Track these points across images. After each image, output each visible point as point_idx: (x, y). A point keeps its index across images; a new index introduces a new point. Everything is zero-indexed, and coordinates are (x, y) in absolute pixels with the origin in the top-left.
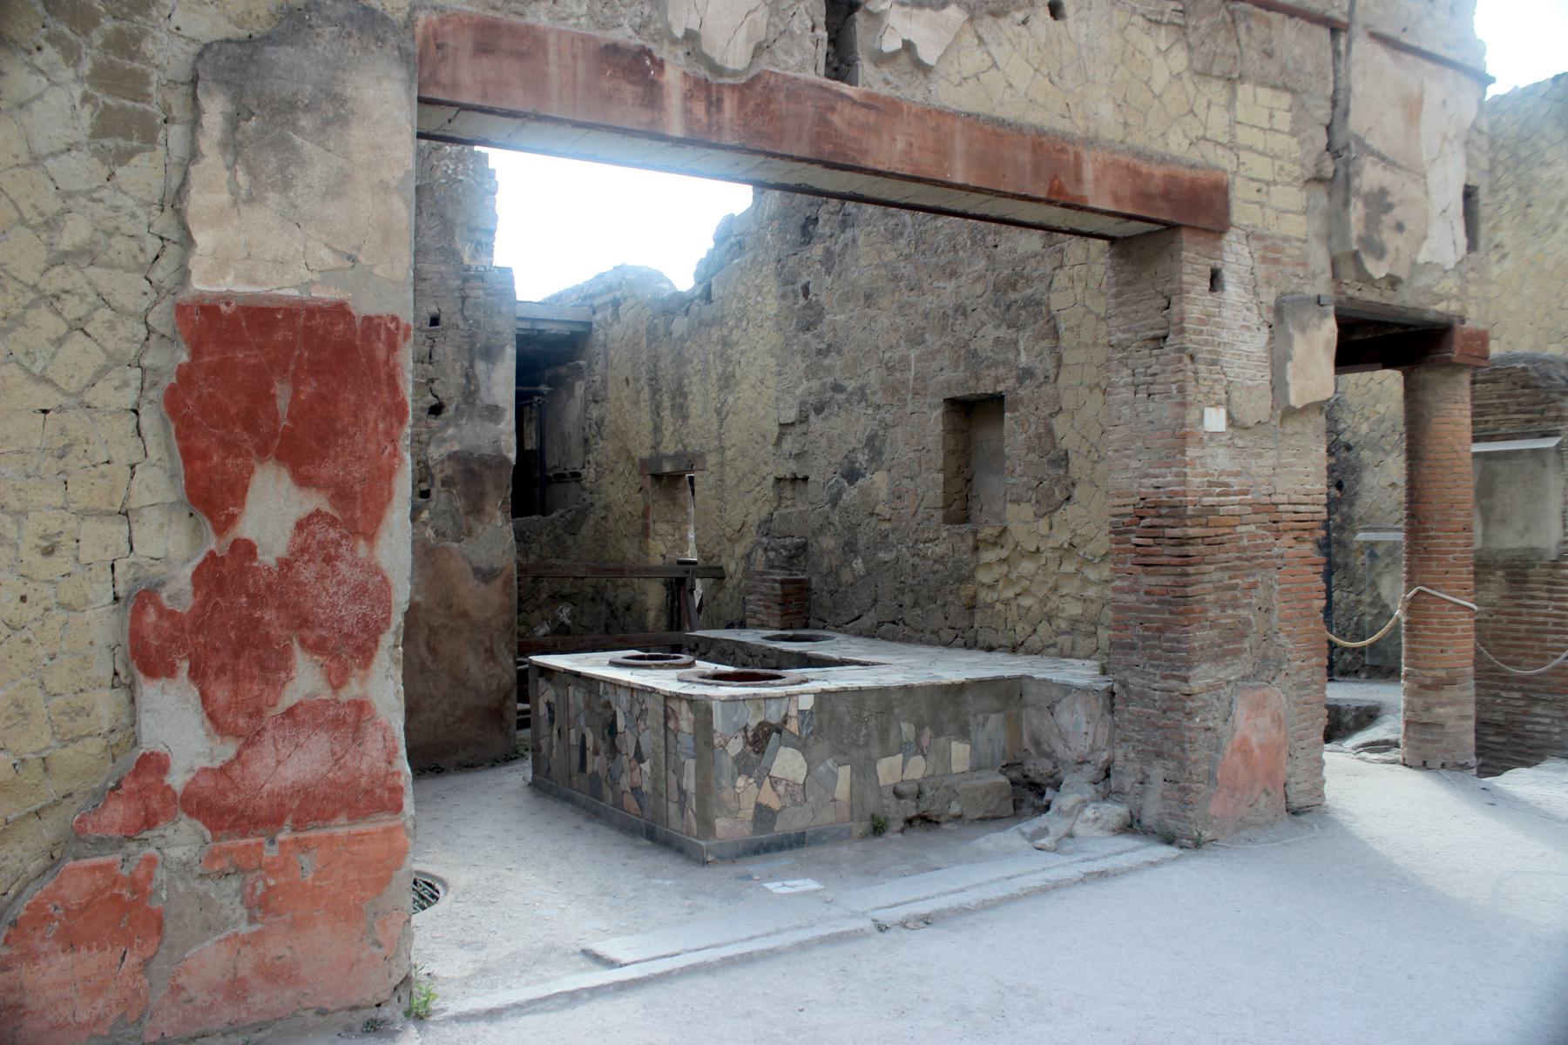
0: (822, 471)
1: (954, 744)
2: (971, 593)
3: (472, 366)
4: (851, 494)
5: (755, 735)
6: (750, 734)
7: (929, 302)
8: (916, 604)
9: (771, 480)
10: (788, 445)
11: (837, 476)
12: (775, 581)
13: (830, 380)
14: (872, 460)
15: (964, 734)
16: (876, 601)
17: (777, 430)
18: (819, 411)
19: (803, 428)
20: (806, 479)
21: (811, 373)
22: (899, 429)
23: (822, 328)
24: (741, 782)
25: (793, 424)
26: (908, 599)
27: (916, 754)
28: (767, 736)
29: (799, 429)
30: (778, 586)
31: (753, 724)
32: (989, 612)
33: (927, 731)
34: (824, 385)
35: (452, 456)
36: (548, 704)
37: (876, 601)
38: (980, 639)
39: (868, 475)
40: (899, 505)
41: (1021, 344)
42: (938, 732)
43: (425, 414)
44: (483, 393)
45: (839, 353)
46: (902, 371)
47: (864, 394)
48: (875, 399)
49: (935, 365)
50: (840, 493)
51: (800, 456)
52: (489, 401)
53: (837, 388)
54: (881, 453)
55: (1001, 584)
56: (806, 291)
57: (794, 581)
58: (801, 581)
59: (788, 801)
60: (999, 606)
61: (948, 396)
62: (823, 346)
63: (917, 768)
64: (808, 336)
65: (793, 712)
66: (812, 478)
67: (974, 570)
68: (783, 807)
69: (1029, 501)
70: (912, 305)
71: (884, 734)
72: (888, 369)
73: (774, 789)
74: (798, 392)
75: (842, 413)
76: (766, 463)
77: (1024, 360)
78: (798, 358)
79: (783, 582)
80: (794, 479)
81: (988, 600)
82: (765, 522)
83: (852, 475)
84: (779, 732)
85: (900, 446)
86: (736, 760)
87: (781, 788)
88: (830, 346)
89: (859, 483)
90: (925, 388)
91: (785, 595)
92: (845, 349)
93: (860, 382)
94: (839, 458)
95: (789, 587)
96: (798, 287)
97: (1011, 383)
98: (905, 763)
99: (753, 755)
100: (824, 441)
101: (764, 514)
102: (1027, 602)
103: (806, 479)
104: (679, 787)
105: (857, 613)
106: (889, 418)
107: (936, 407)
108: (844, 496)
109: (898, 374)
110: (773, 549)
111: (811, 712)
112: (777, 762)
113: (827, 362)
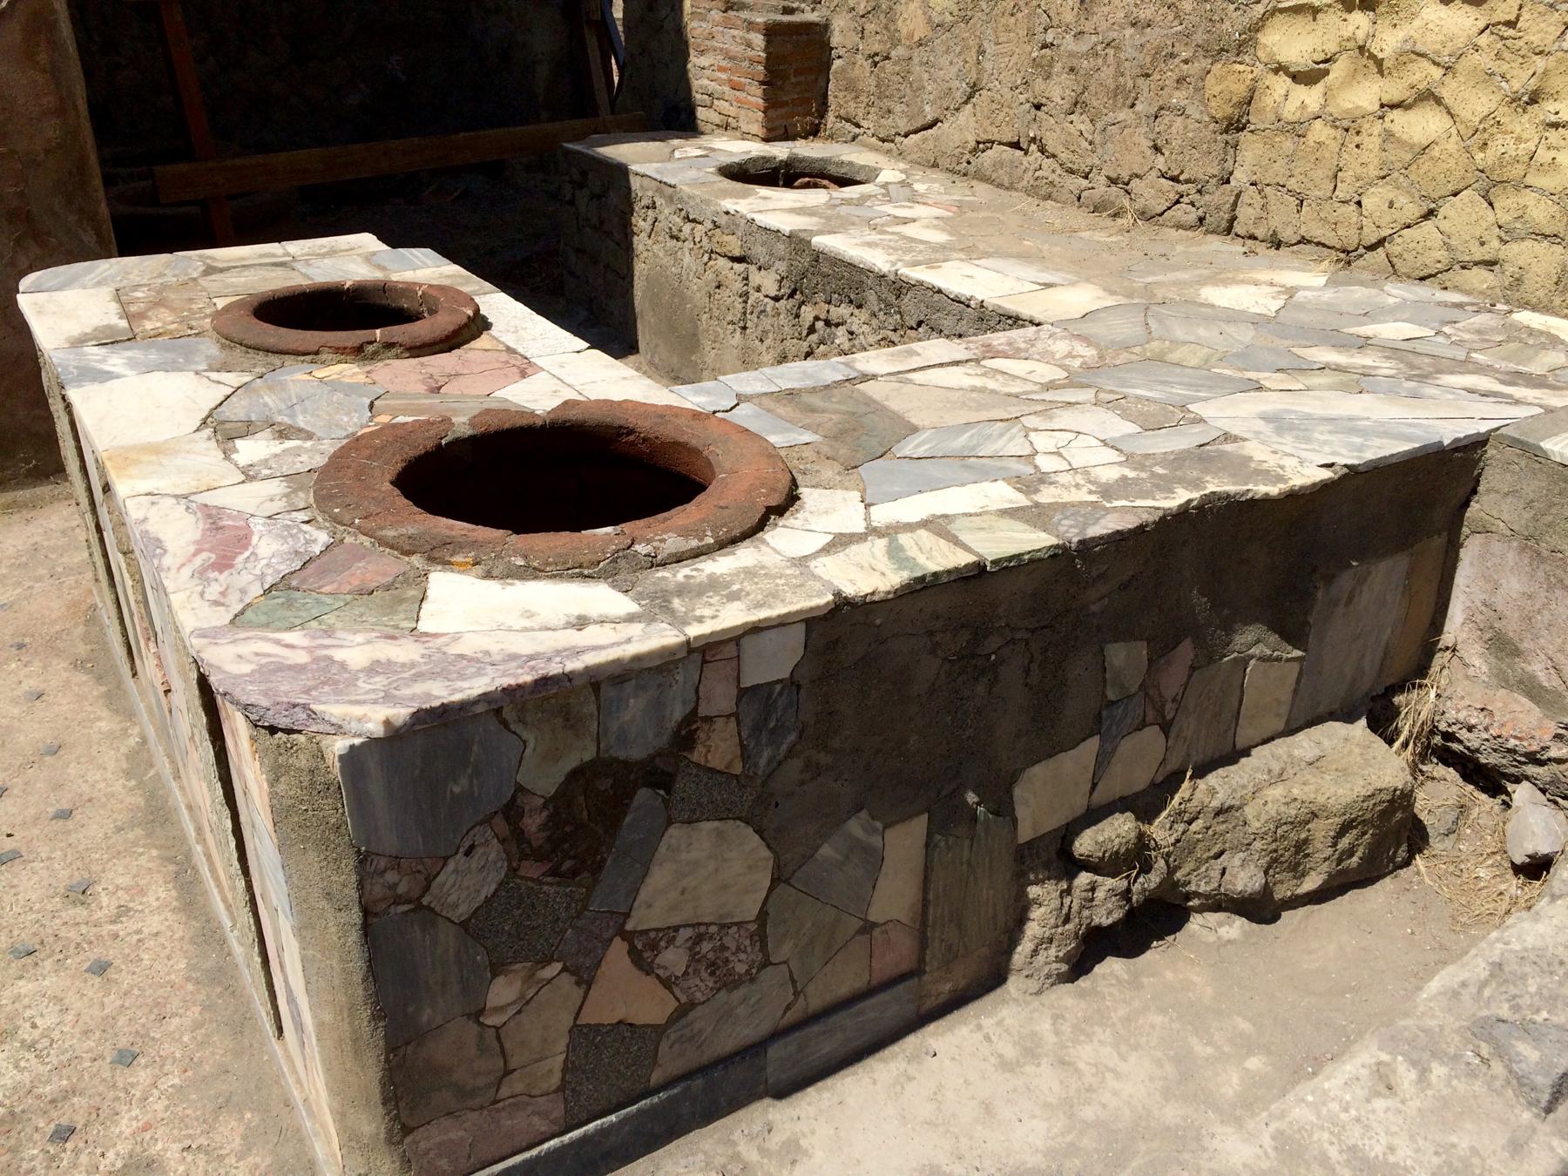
2: (1240, 90)
5: (553, 822)
6: (533, 823)
8: (1077, 105)
12: (750, 26)
16: (975, 89)
24: (503, 991)
26: (1058, 90)
27: (1143, 725)
28: (613, 808)
31: (543, 779)
32: (1288, 144)
37: (975, 89)
55: (1337, 71)
58: (809, 27)
59: (702, 984)
60: (1319, 131)
65: (719, 699)
67: (1257, 27)
81: (1290, 111)
87: (673, 959)
102: (1422, 125)
105: (930, 113)
111: (792, 683)
112: (659, 877)
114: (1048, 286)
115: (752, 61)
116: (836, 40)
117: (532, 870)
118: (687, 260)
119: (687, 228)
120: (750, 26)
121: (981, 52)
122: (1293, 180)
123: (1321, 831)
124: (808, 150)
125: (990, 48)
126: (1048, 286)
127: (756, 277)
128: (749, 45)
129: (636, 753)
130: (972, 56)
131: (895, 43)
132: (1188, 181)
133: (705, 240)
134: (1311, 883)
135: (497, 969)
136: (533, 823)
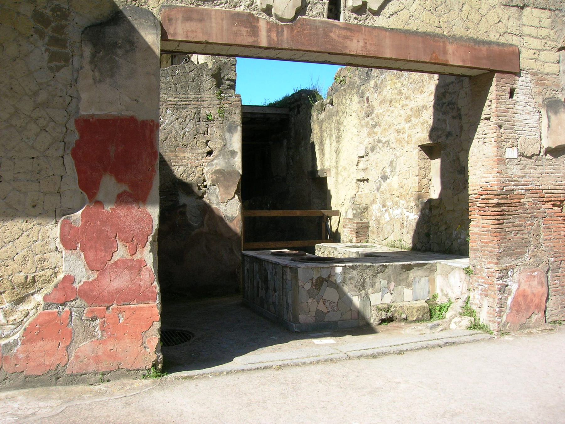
0: (373, 176)
1: (405, 290)
3: (224, 135)
4: (384, 186)
5: (316, 282)
6: (314, 282)
7: (412, 104)
9: (355, 180)
10: (361, 166)
11: (380, 179)
13: (376, 138)
14: (392, 171)
15: (409, 286)
16: (393, 231)
18: (372, 150)
20: (367, 180)
21: (369, 134)
23: (373, 115)
24: (310, 301)
25: (363, 157)
28: (322, 283)
29: (366, 158)
30: (355, 225)
31: (315, 277)
33: (393, 284)
34: (374, 140)
35: (217, 172)
36: (248, 270)
37: (393, 231)
38: (432, 247)
39: (391, 178)
40: (401, 190)
41: (447, 121)
42: (398, 284)
43: (205, 155)
44: (228, 146)
45: (380, 126)
47: (389, 143)
49: (415, 131)
50: (380, 185)
51: (365, 169)
52: (231, 149)
53: (379, 141)
54: (395, 169)
56: (368, 99)
59: (330, 310)
62: (374, 123)
63: (388, 299)
64: (368, 119)
68: (328, 312)
69: (450, 189)
70: (407, 105)
71: (373, 285)
72: (398, 132)
73: (324, 304)
74: (365, 143)
77: (448, 129)
78: (365, 128)
79: (357, 223)
82: (353, 198)
83: (385, 178)
84: (327, 281)
85: (401, 165)
86: (308, 291)
87: (327, 304)
88: (376, 123)
89: (386, 181)
90: (411, 141)
92: (382, 125)
95: (360, 225)
96: (365, 98)
97: (444, 138)
98: (383, 296)
99: (315, 290)
100: (374, 164)
101: (352, 195)
103: (367, 180)
104: (287, 302)
106: (398, 154)
107: (415, 149)
108: (382, 187)
109: (401, 135)
110: (355, 209)
113: (375, 130)
117: (314, 287)
120: (354, 223)
123: (415, 310)
129: (324, 277)
134: (415, 319)
135: (310, 298)
136: (314, 282)
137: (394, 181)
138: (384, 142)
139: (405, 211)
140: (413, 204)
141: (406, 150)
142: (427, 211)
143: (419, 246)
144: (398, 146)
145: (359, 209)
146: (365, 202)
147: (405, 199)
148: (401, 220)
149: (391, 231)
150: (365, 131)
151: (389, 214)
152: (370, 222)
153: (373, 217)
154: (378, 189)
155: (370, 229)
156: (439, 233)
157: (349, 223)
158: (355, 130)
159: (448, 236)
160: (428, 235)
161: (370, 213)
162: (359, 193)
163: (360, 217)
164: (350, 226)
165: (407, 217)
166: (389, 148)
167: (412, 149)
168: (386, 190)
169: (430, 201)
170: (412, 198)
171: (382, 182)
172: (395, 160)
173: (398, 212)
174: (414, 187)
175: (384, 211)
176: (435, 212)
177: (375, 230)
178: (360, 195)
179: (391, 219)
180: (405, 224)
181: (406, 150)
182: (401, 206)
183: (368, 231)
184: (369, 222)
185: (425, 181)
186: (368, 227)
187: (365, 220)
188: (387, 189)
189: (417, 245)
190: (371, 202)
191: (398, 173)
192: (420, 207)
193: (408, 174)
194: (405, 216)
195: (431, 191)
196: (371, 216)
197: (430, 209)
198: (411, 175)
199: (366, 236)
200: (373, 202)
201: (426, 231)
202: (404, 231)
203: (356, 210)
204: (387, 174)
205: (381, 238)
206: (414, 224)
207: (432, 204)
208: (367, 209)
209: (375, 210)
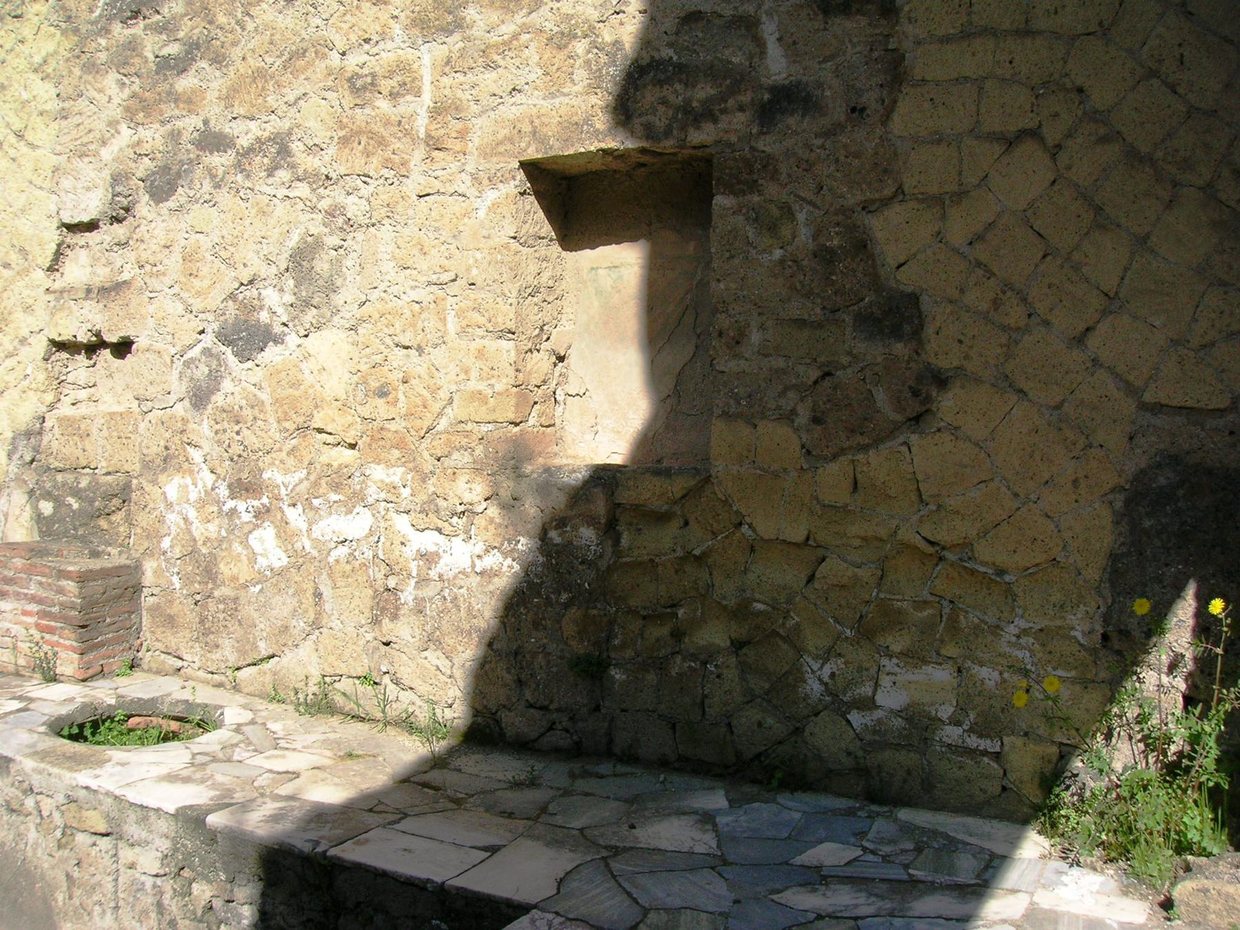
0: (168, 323)
4: (241, 380)
9: (39, 346)
10: (77, 270)
11: (208, 340)
12: (63, 574)
17: (52, 237)
19: (120, 231)
20: (123, 348)
21: (139, 109)
22: (386, 232)
25: (92, 226)
29: (108, 234)
30: (70, 586)
34: (175, 136)
37: (316, 625)
39: (292, 340)
40: (380, 408)
41: (769, 30)
45: (218, 60)
46: (394, 96)
47: (284, 151)
48: (309, 163)
50: (215, 379)
51: (110, 291)
53: (212, 141)
54: (331, 288)
57: (105, 573)
58: (118, 571)
61: (533, 153)
62: (173, 49)
64: (138, 28)
66: (140, 343)
69: (789, 417)
72: (356, 91)
75: (224, 197)
76: (28, 309)
77: (777, 66)
78: (111, 78)
79: (83, 578)
80: (92, 348)
82: (28, 434)
83: (247, 337)
85: (378, 268)
90: (462, 135)
91: (89, 605)
92: (236, 53)
93: (276, 125)
94: (215, 299)
95: (97, 586)
97: (737, 123)
100: (173, 262)
105: (264, 649)
106: (355, 207)
107: (494, 180)
108: (227, 385)
109: (383, 105)
110: (48, 496)
113: (185, 83)
114: (493, 850)
115: (63, 605)
116: (148, 578)
118: (32, 835)
119: (30, 802)
120: (63, 574)
121: (318, 595)
122: (663, 706)
124: (137, 687)
125: (327, 591)
126: (493, 850)
127: (127, 854)
128: (61, 591)
130: (309, 600)
131: (217, 586)
132: (558, 710)
133: (57, 815)
137: (324, 359)
138: (244, 142)
139: (402, 523)
140: (472, 490)
141: (412, 186)
142: (587, 534)
143: (515, 722)
144: (359, 164)
145: (76, 493)
146: (104, 455)
147: (409, 459)
148: (378, 573)
149: (300, 625)
150: (112, 91)
151: (285, 535)
152: (149, 566)
153: (166, 543)
154: (200, 397)
155: (147, 601)
156: (678, 665)
157: (30, 571)
158: (44, 92)
159: (759, 684)
160: (593, 669)
161: (143, 519)
162: (65, 409)
163: (84, 540)
164: (33, 590)
165: (429, 558)
166: (283, 175)
167: (463, 184)
168: (256, 404)
169: (603, 477)
170: (460, 459)
171: (232, 359)
172: (334, 241)
173: (357, 524)
174: (478, 396)
175: (246, 517)
176: (645, 543)
177: (185, 610)
178: (66, 422)
179: (299, 561)
180: (408, 595)
181: (412, 186)
182: (372, 493)
183: (135, 609)
184: (137, 568)
185: (540, 363)
186: (137, 589)
187: (114, 557)
188: (264, 396)
189: (506, 718)
190: (147, 465)
191: (351, 312)
192: (531, 508)
193: (431, 323)
194: (409, 552)
195: (571, 418)
196: (154, 535)
197: (610, 529)
198: (452, 326)
199: (129, 633)
200: (169, 461)
201: (580, 648)
202: (405, 630)
203: (58, 502)
204: (264, 316)
205: (228, 652)
206: (484, 609)
207: (626, 496)
208: (123, 494)
209: (181, 503)
